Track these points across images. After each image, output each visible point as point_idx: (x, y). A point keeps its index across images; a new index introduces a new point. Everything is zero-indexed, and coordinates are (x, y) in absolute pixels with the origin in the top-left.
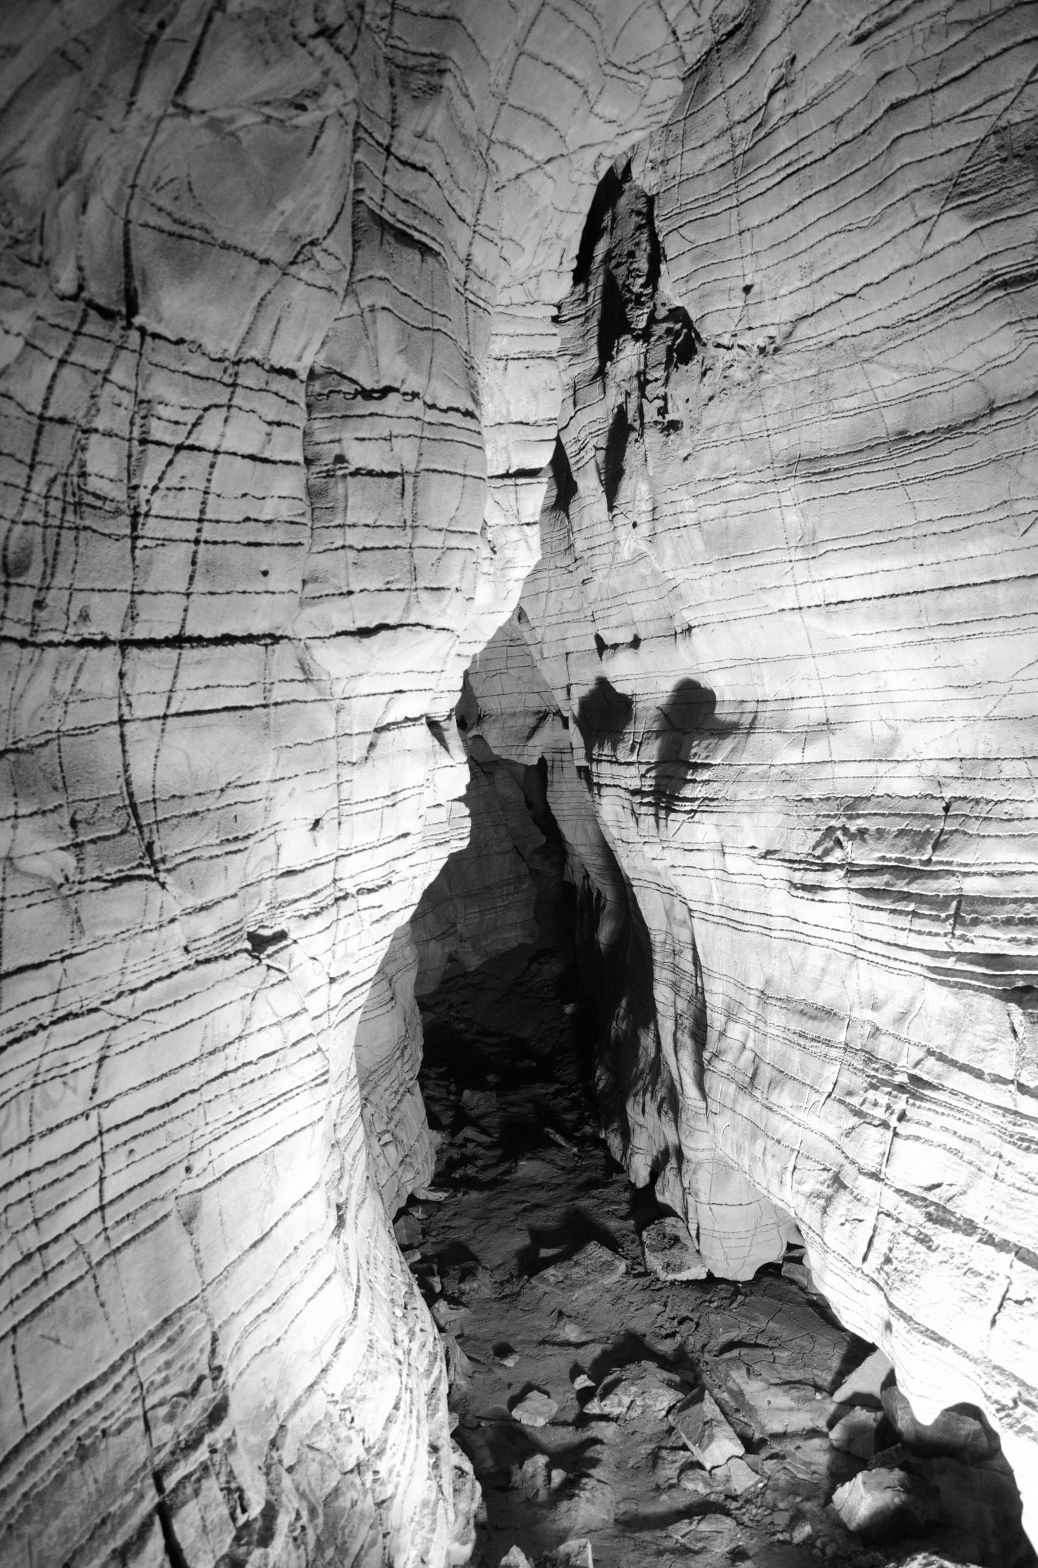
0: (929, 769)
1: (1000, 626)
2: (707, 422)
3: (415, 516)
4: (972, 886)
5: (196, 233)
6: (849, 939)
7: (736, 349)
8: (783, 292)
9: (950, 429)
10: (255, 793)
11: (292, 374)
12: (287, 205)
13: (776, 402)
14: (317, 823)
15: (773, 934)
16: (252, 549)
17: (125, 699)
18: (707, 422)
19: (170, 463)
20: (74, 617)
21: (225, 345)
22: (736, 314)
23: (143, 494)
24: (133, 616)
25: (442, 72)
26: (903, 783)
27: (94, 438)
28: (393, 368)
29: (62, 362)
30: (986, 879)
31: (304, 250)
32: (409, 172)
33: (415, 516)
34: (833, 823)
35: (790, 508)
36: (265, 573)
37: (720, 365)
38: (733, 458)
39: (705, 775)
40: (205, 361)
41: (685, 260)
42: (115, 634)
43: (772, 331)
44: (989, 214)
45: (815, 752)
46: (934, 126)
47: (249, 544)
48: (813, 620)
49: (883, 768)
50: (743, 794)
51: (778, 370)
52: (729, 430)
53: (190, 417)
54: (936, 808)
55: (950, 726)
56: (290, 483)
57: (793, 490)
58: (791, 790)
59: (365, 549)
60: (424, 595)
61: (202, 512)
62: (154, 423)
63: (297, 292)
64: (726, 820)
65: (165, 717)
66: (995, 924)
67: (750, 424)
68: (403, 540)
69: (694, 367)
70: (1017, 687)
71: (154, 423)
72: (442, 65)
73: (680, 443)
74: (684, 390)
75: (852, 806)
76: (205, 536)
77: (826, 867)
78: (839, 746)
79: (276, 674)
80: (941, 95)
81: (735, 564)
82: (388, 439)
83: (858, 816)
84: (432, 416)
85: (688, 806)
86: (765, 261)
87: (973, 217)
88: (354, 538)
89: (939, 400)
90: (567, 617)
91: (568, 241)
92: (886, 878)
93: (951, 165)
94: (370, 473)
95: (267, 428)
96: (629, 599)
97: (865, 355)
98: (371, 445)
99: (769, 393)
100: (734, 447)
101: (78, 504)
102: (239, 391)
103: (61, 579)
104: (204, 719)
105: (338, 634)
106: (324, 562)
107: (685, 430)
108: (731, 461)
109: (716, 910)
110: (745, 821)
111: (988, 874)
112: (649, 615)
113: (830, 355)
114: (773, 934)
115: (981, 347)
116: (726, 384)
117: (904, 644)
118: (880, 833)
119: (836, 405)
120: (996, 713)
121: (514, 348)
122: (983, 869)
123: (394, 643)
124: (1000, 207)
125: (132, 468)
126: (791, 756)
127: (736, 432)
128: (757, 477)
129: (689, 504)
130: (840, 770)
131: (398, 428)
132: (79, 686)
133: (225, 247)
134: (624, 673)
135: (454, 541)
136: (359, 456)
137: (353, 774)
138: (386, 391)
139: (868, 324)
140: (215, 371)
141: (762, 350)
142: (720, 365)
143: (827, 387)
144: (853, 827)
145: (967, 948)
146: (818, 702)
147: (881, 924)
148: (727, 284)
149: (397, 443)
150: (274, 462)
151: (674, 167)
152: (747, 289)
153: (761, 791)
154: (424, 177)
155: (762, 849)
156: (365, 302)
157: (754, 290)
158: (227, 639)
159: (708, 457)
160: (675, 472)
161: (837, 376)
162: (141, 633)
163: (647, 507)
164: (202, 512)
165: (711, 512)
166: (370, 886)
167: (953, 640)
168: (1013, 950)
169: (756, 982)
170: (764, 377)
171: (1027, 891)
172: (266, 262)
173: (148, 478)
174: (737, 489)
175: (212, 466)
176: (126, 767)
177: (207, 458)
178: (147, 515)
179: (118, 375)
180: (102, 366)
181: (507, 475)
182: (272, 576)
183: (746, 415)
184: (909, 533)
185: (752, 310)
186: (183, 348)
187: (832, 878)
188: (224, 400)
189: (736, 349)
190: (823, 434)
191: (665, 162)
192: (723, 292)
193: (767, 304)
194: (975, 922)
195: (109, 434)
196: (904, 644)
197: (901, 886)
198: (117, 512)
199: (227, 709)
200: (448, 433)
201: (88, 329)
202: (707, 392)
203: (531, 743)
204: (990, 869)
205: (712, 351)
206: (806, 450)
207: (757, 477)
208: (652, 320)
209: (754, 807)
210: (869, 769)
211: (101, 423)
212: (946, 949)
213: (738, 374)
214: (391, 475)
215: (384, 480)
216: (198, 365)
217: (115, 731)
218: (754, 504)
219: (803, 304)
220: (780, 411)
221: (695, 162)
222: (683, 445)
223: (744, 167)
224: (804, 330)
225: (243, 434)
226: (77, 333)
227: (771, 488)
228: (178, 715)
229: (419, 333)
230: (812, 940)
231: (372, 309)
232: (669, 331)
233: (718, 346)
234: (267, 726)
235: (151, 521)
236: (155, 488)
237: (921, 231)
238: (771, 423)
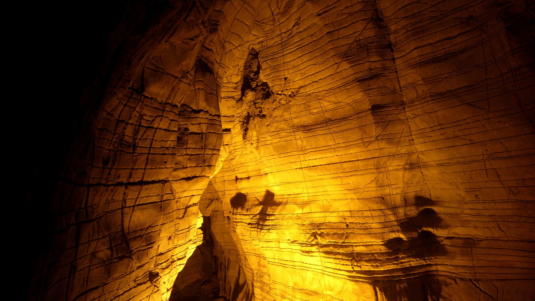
0: (341, 214)
1: (360, 172)
2: (274, 115)
4: (358, 249)
5: (161, 70)
6: (320, 268)
8: (296, 80)
9: (344, 118)
10: (156, 229)
11: (176, 106)
12: (184, 63)
13: (294, 110)
14: (170, 238)
15: (296, 268)
16: (162, 156)
17: (124, 201)
18: (274, 115)
19: (145, 132)
20: (116, 177)
21: (163, 99)
22: (282, 85)
23: (137, 141)
24: (130, 176)
25: (218, 25)
26: (333, 218)
27: (129, 125)
28: (203, 105)
29: (125, 105)
30: (362, 247)
31: (185, 74)
32: (207, 51)
33: (205, 145)
34: (314, 231)
36: (166, 162)
37: (278, 100)
38: (283, 125)
39: (273, 218)
40: (157, 104)
41: (268, 70)
42: (125, 181)
43: (293, 90)
44: (355, 62)
45: (306, 210)
46: (339, 39)
47: (162, 154)
48: (305, 171)
49: (327, 214)
50: (285, 223)
51: (295, 101)
52: (281, 117)
53: (151, 119)
54: (344, 226)
55: (347, 201)
56: (173, 137)
57: (300, 135)
58: (299, 222)
59: (192, 155)
60: (207, 168)
61: (151, 145)
62: (143, 121)
63: (182, 85)
64: (280, 231)
65: (134, 206)
66: (366, 261)
67: (287, 116)
69: (270, 100)
70: (366, 189)
71: (143, 121)
72: (218, 23)
73: (266, 121)
74: (267, 106)
75: (319, 226)
76: (151, 152)
77: (312, 245)
78: (314, 208)
79: (165, 192)
80: (341, 31)
81: (283, 155)
82: (199, 124)
83: (321, 229)
85: (268, 228)
86: (291, 71)
87: (350, 63)
88: (189, 152)
89: (341, 110)
90: (225, 170)
91: (240, 66)
92: (331, 248)
93: (344, 49)
95: (170, 122)
96: (247, 165)
97: (320, 98)
98: (195, 126)
100: (282, 122)
101: (121, 144)
102: (165, 112)
103: (115, 167)
104: (144, 206)
105: (181, 179)
106: (180, 158)
107: (267, 117)
108: (282, 126)
109: (276, 261)
110: (286, 232)
111: (363, 246)
112: (253, 169)
113: (310, 97)
114: (296, 268)
115: (353, 97)
116: (279, 105)
117: (332, 178)
118: (328, 234)
119: (312, 111)
120: (360, 197)
122: (361, 244)
123: (197, 182)
124: (358, 61)
125: (136, 132)
126: (299, 211)
127: (282, 118)
128: (289, 131)
129: (269, 138)
130: (314, 215)
132: (114, 198)
133: (167, 74)
134: (244, 187)
137: (181, 222)
138: (199, 111)
139: (321, 89)
141: (290, 96)
142: (278, 100)
143: (309, 106)
144: (319, 232)
145: (357, 269)
146: (306, 195)
147: (331, 263)
149: (202, 125)
150: (171, 131)
153: (291, 222)
154: (211, 52)
155: (292, 240)
156: (197, 87)
157: (288, 79)
158: (154, 182)
159: (275, 125)
160: (264, 129)
161: (311, 104)
162: (132, 181)
163: (255, 139)
164: (151, 145)
165: (275, 141)
166: (181, 257)
167: (347, 176)
168: (372, 269)
169: (291, 284)
170: (291, 103)
171: (375, 250)
172: (176, 77)
175: (155, 132)
176: (122, 221)
177: (154, 130)
178: (137, 146)
179: (138, 109)
180: (134, 106)
182: (168, 163)
183: (285, 114)
184: (333, 147)
185: (287, 85)
186: (153, 100)
187: (314, 249)
188: (161, 114)
192: (279, 79)
194: (360, 261)
195: (132, 124)
196: (332, 178)
197: (336, 250)
198: (130, 146)
199: (151, 203)
201: (133, 96)
202: (274, 107)
203: (208, 209)
204: (363, 244)
205: (276, 96)
206: (303, 123)
207: (289, 131)
208: (257, 86)
209: (289, 227)
210: (322, 215)
211: (130, 122)
212: (352, 269)
213: (283, 102)
214: (199, 134)
215: (198, 136)
216: (155, 105)
217: (120, 211)
218: (288, 138)
219: (301, 83)
220: (295, 112)
222: (267, 122)
223: (285, 45)
224: (302, 91)
225: (164, 124)
226: (130, 97)
228: (138, 205)
229: (209, 95)
230: (309, 269)
231: (199, 89)
232: (262, 89)
233: (278, 94)
234: (161, 207)
235: (138, 148)
236: (140, 139)
237: (336, 66)
238: (292, 116)
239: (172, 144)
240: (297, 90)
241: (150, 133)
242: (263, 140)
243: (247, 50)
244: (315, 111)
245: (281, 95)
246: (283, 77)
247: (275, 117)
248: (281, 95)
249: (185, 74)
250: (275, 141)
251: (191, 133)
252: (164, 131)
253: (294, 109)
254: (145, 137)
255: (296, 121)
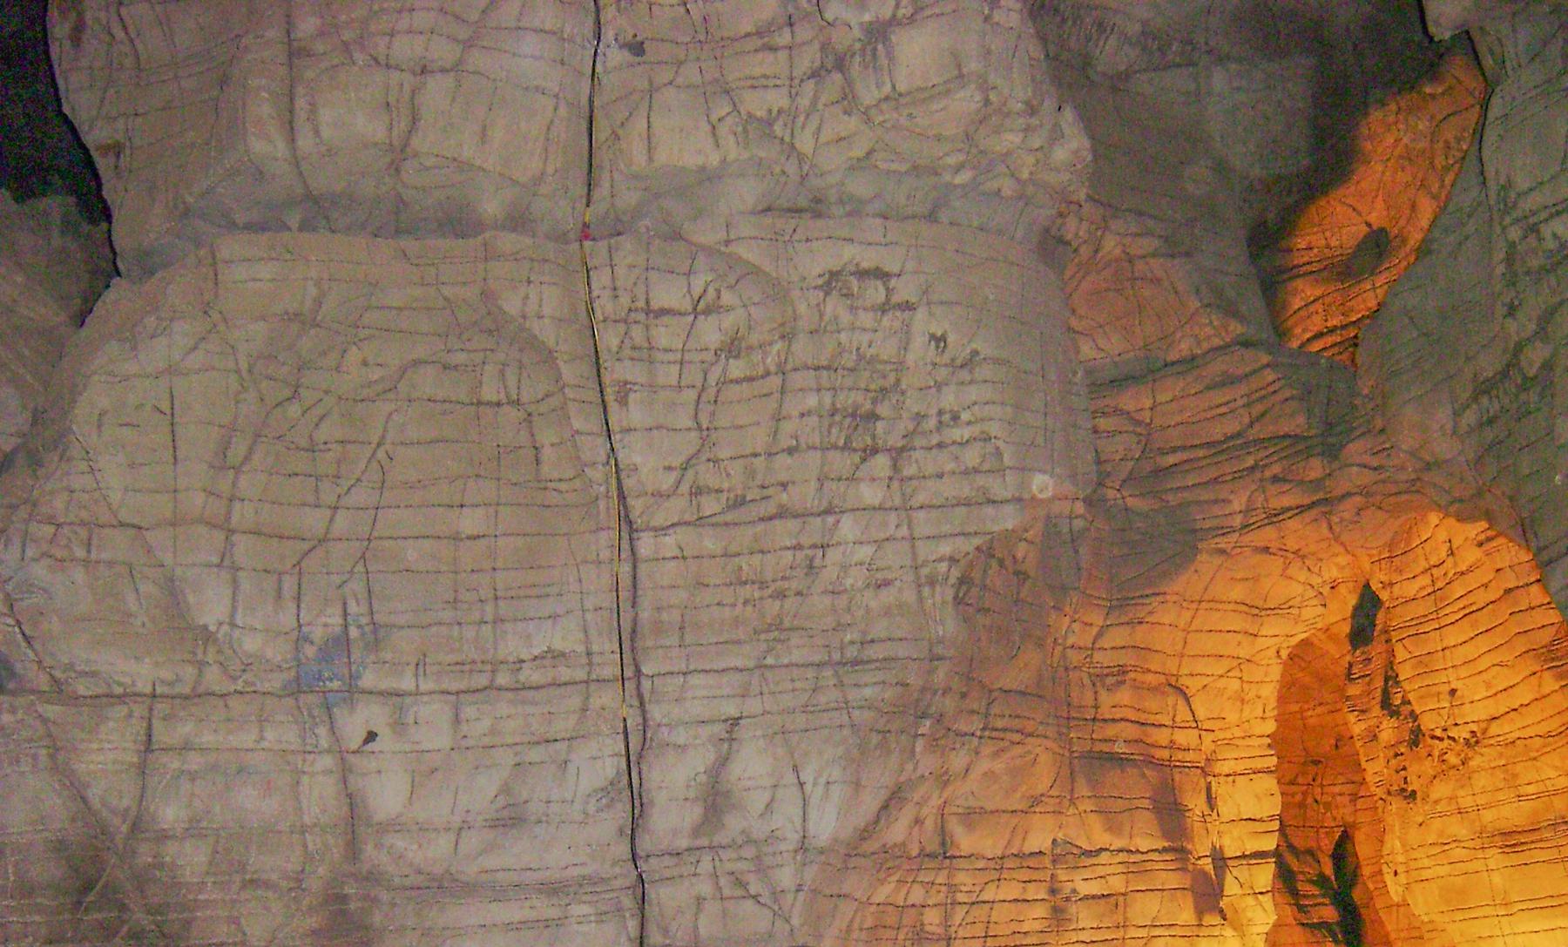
3: (1126, 919)
7: (1446, 742)
18: (1434, 796)
28: (1102, 838)
35: (1496, 869)
37: (1436, 753)
41: (1408, 666)
43: (1474, 727)
53: (977, 889)
56: (1040, 911)
57: (1495, 858)
68: (1120, 934)
69: (1421, 751)
73: (1418, 812)
81: (1459, 916)
84: (1133, 858)
94: (1094, 897)
97: (1533, 754)
99: (1476, 776)
113: (1509, 751)
119: (1522, 790)
121: (1240, 767)
128: (1470, 844)
131: (1109, 870)
135: (1157, 932)
136: (1085, 889)
140: (992, 864)
142: (1436, 753)
148: (1434, 689)
151: (1396, 589)
152: (1453, 692)
156: (1081, 808)
157: (1458, 693)
159: (1437, 824)
160: (1414, 836)
161: (1519, 768)
165: (1442, 871)
170: (1472, 763)
173: (957, 919)
174: (1459, 853)
181: (1244, 856)
183: (1461, 793)
189: (1446, 742)
190: (1512, 814)
191: (1391, 584)
193: (1467, 706)
200: (1149, 866)
202: (1432, 772)
206: (1506, 826)
215: (1102, 901)
216: (981, 864)
221: (1411, 589)
223: (1442, 599)
224: (1495, 729)
225: (1011, 891)
227: (1480, 854)
233: (1433, 737)
238: (1481, 800)
239: (1037, 926)
240: (1484, 725)
241: (980, 913)
242: (1413, 865)
243: (1275, 661)
244: (1531, 789)
245: (1441, 739)
246: (1447, 688)
247: (1436, 802)
248: (1441, 739)
249: (1036, 800)
250: (1442, 871)
251: (1086, 897)
252: (1013, 905)
253: (1481, 781)
254: (970, 919)
255: (1488, 816)
